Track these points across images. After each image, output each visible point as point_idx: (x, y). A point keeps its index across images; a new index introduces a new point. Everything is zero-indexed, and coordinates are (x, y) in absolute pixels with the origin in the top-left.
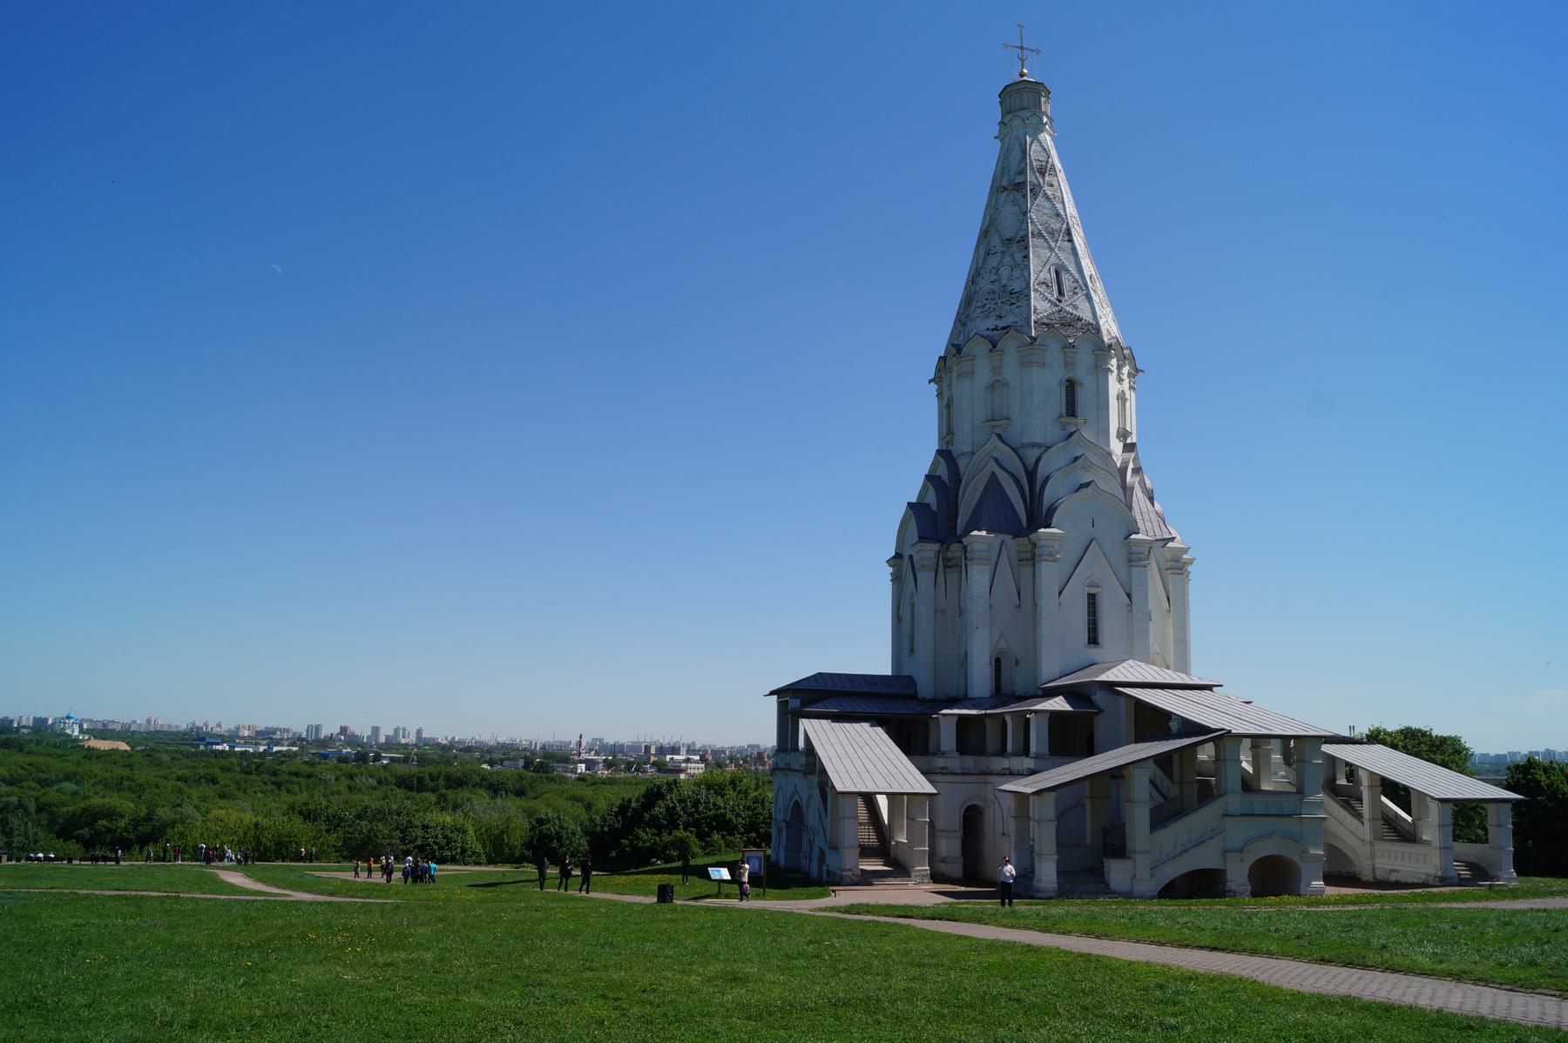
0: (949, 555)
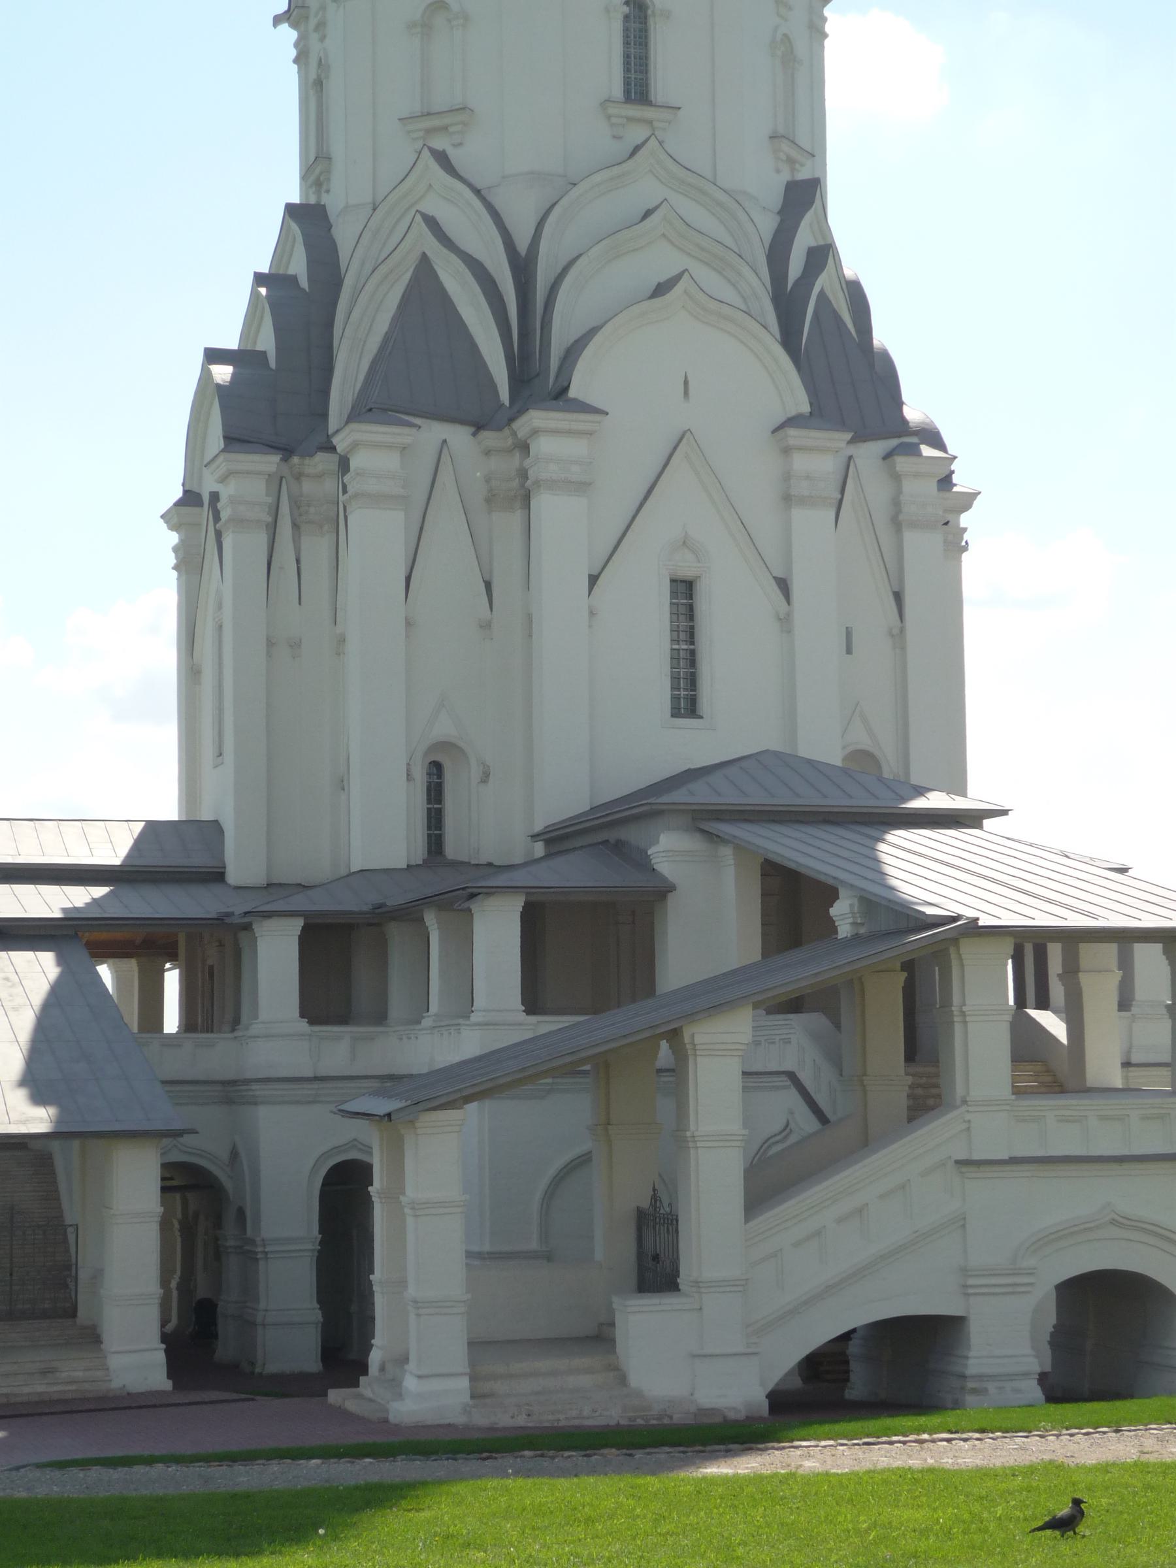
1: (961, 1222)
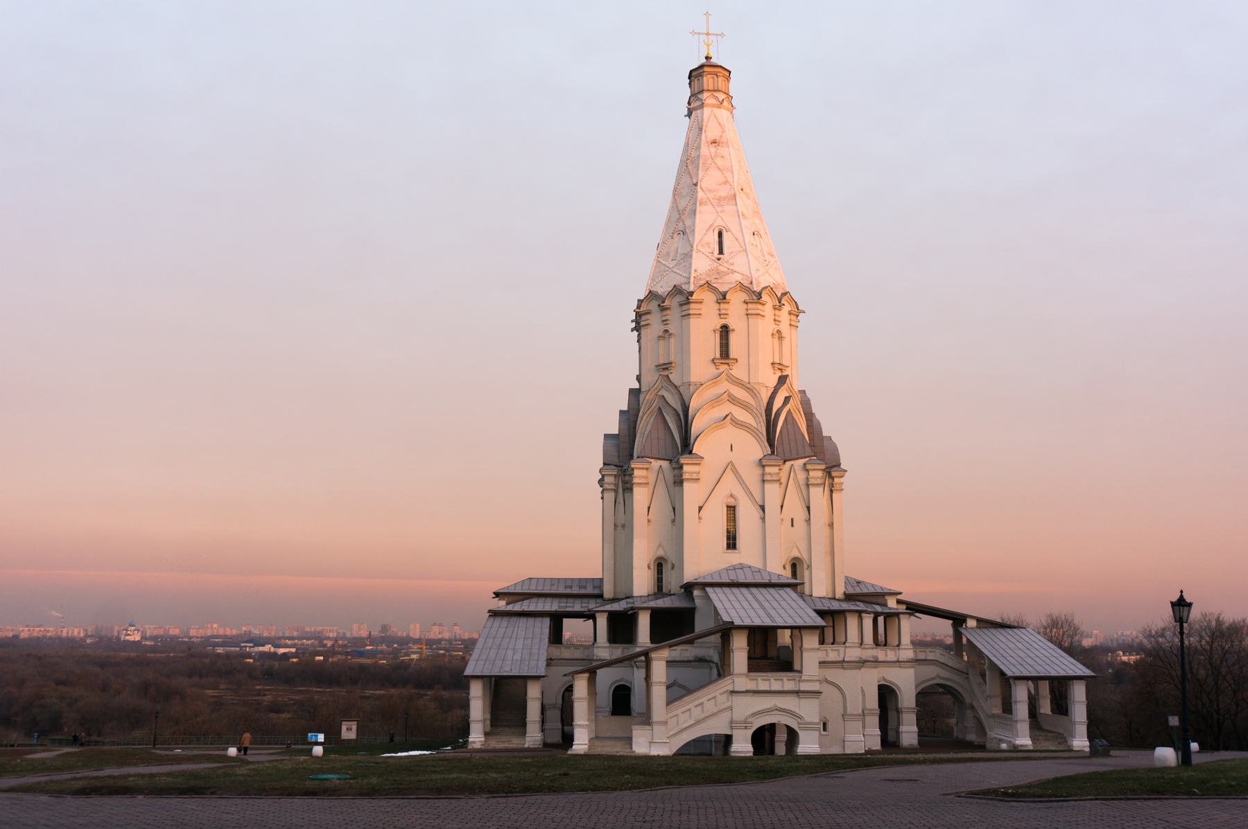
0: (627, 478)
1: (731, 708)
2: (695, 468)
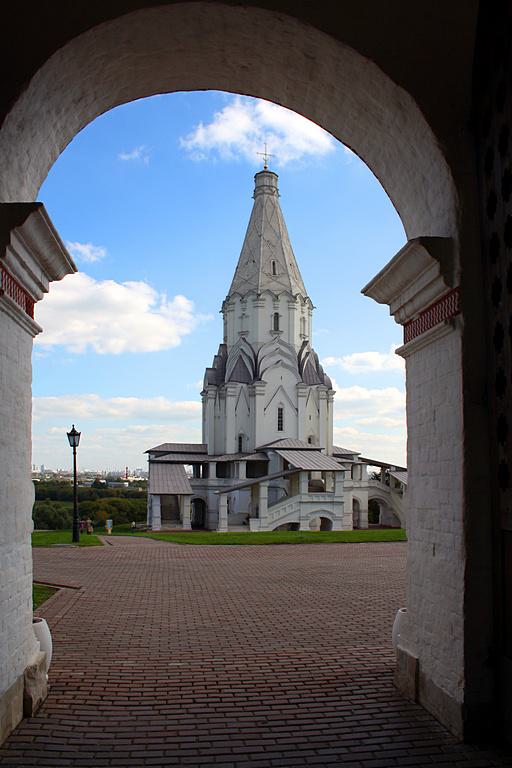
2: (262, 388)
